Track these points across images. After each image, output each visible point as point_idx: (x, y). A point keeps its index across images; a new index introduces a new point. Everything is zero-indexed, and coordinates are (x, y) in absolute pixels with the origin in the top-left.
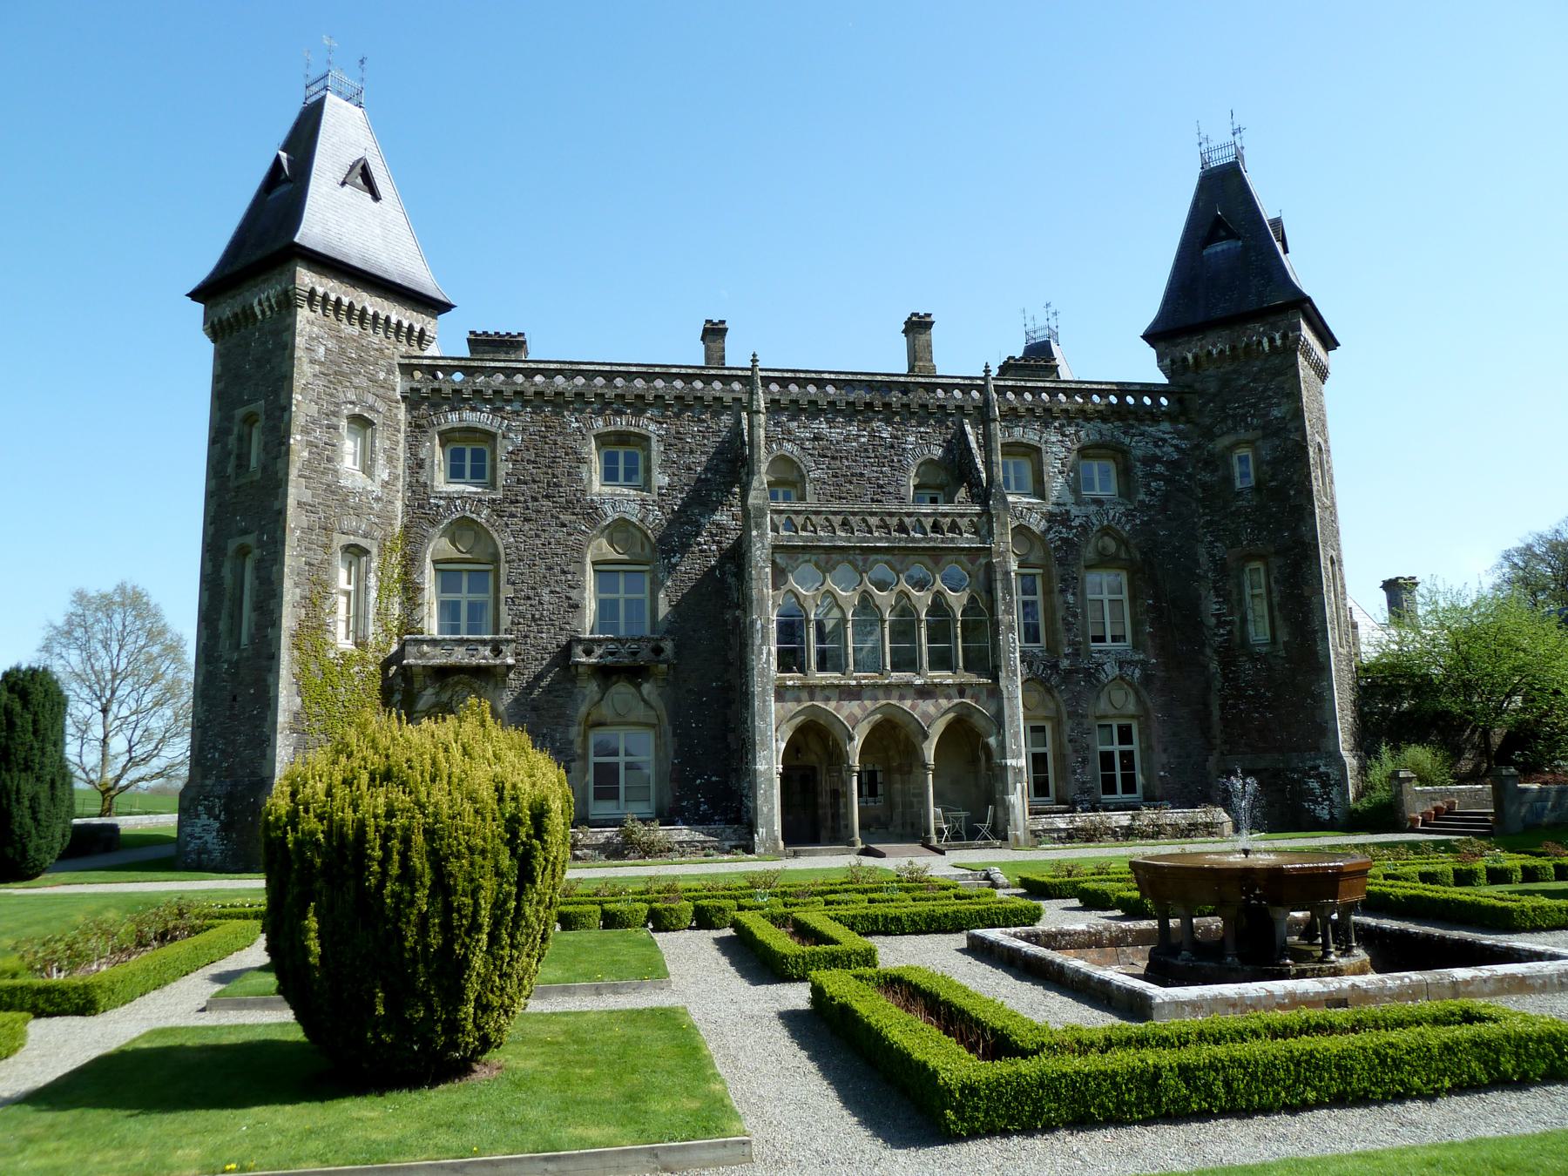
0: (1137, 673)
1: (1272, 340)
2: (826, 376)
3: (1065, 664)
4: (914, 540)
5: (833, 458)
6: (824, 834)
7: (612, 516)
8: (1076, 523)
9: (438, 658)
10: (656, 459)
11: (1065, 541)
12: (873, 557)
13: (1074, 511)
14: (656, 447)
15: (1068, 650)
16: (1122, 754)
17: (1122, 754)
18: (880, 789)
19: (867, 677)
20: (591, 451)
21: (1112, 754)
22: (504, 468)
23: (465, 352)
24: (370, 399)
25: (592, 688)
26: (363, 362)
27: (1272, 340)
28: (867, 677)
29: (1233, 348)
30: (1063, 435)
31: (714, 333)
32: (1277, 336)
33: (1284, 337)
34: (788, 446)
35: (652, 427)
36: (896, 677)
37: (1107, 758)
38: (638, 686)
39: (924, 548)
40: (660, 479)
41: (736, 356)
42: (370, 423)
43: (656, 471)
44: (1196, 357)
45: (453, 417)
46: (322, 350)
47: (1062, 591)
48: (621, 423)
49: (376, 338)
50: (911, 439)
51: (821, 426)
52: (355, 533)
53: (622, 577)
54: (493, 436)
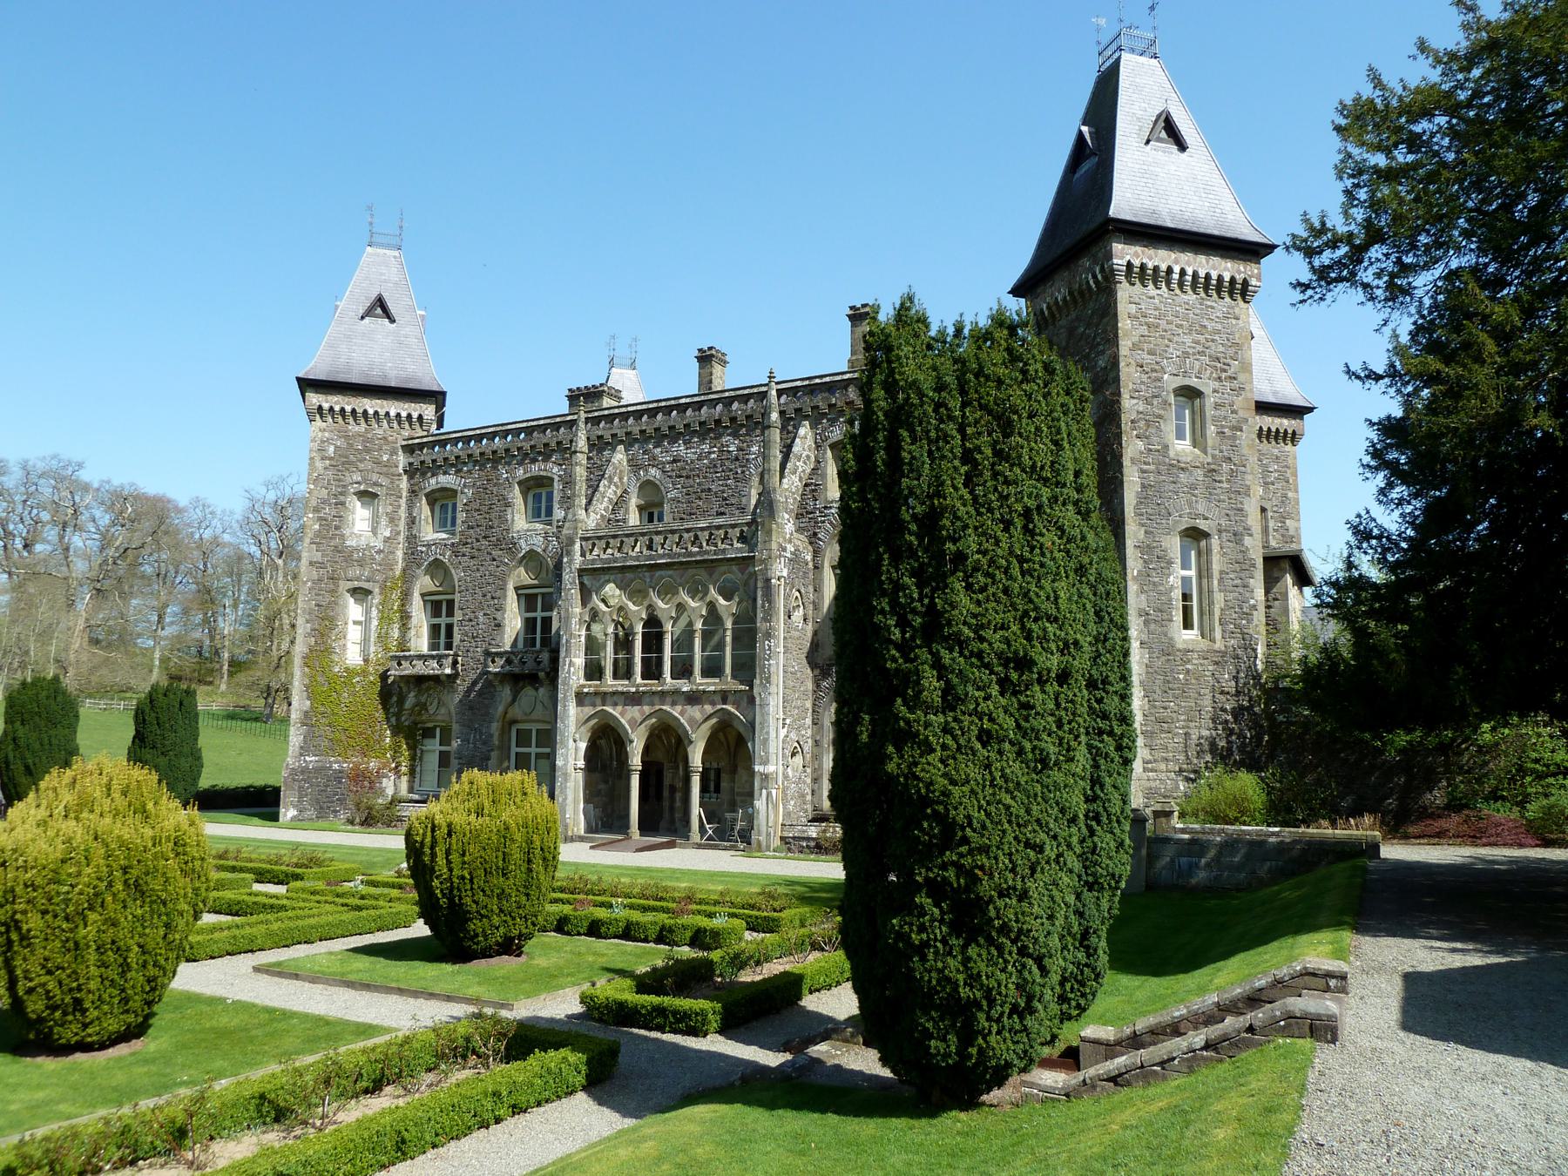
1: (1095, 277)
2: (683, 401)
4: (691, 554)
5: (688, 477)
6: (663, 824)
7: (525, 548)
9: (420, 668)
12: (658, 573)
18: (724, 785)
19: (711, 684)
20: (516, 495)
22: (461, 516)
24: (375, 477)
25: (506, 692)
26: (368, 450)
27: (1095, 277)
28: (711, 684)
29: (1071, 293)
31: (706, 358)
33: (1102, 270)
34: (653, 471)
35: (555, 470)
41: (727, 379)
42: (375, 496)
43: (556, 506)
44: (1049, 308)
45: (433, 481)
46: (332, 449)
49: (379, 431)
50: (755, 449)
51: (680, 448)
52: (358, 579)
54: (455, 492)
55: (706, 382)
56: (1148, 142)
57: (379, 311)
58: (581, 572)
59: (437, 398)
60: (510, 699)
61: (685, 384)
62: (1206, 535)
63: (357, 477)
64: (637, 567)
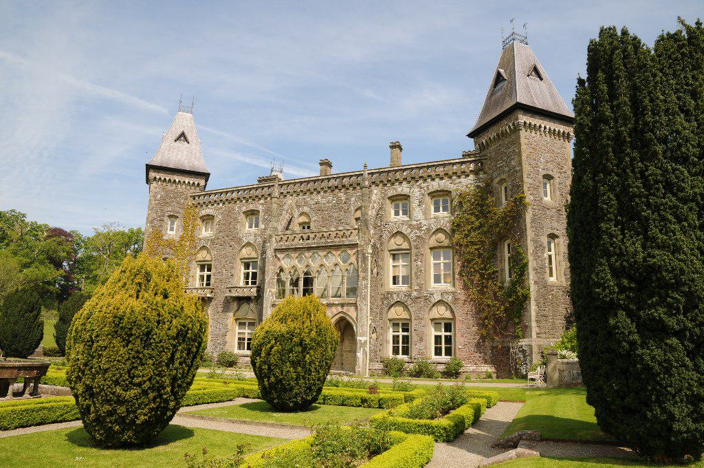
0: (450, 297)
1: (509, 127)
3: (415, 294)
8: (424, 228)
10: (261, 219)
11: (418, 237)
13: (424, 222)
14: (261, 214)
15: (417, 288)
16: (446, 336)
17: (446, 336)
21: (440, 337)
23: (257, 183)
24: (177, 209)
27: (509, 127)
30: (421, 188)
31: (326, 164)
32: (511, 125)
33: (514, 124)
35: (261, 207)
36: (347, 300)
37: (438, 338)
38: (249, 304)
39: (332, 246)
40: (262, 226)
41: (334, 171)
43: (260, 223)
44: (486, 141)
46: (159, 196)
47: (415, 260)
48: (251, 207)
50: (353, 199)
53: (401, 256)
55: (323, 172)
56: (528, 76)
57: (182, 138)
58: (276, 250)
59: (206, 176)
60: (236, 308)
61: (314, 172)
62: (557, 237)
63: (170, 209)
64: (302, 248)
